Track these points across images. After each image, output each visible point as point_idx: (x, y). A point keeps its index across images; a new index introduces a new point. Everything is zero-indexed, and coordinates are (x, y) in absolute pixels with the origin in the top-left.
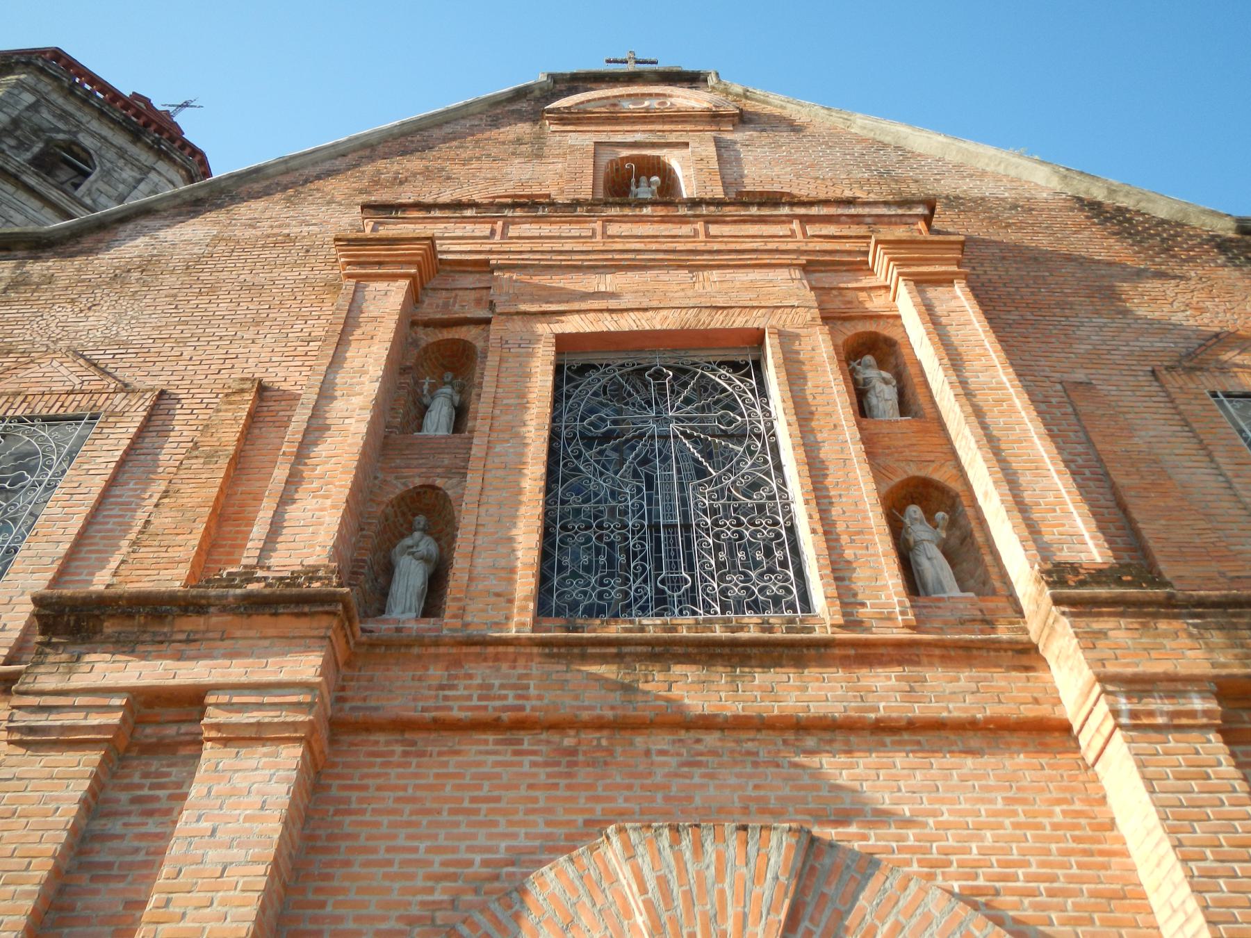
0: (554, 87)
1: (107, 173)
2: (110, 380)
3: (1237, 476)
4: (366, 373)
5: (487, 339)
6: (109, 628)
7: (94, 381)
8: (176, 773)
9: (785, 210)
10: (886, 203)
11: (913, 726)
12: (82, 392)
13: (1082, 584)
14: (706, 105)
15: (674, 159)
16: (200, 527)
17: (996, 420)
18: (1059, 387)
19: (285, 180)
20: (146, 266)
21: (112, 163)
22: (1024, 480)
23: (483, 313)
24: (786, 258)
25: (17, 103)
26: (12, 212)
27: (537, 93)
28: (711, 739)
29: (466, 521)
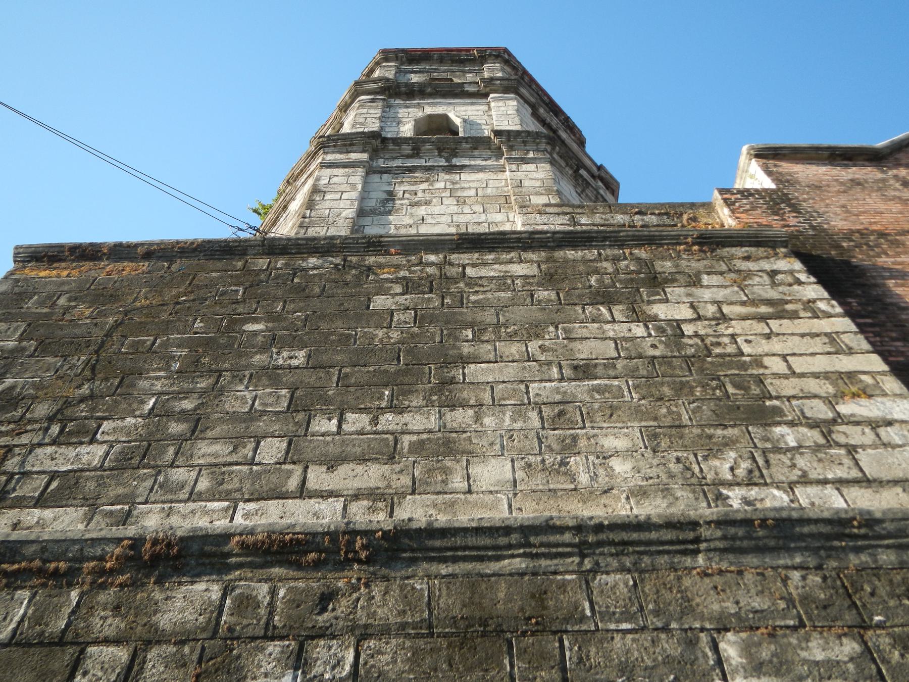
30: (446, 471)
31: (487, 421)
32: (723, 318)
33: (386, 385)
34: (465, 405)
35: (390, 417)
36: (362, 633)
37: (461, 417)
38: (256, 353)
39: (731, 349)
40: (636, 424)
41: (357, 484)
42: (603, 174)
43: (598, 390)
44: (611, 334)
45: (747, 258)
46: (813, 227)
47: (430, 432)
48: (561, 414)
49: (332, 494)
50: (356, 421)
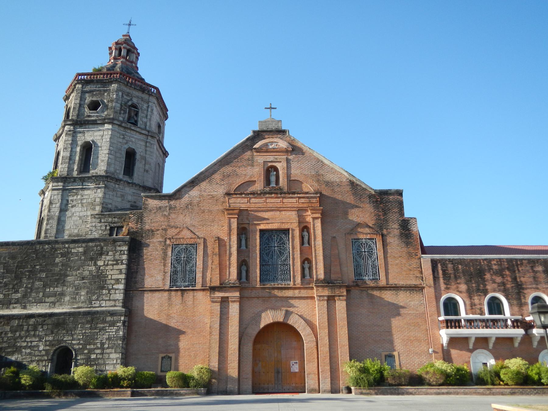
0: (254, 134)
1: (141, 109)
2: (195, 236)
3: (348, 257)
4: (234, 242)
5: (249, 227)
6: (216, 289)
7: (194, 237)
8: (227, 304)
9: (296, 195)
10: (313, 193)
11: (299, 297)
12: (192, 238)
13: (318, 283)
14: (285, 147)
15: (278, 165)
16: (218, 268)
17: (317, 252)
18: (331, 238)
19: (207, 174)
20: (191, 204)
22: (318, 263)
23: (248, 222)
25: (119, 97)
26: (132, 139)
27: (251, 138)
28: (278, 298)
30: (62, 299)
31: (68, 289)
32: (108, 265)
33: (56, 282)
34: (66, 286)
35: (56, 288)
36: (48, 325)
37: (65, 288)
38: (39, 274)
39: (105, 273)
40: (86, 290)
41: (51, 301)
42: (150, 134)
43: (84, 283)
44: (90, 269)
45: (119, 246)
46: (141, 229)
47: (60, 291)
48: (78, 288)
49: (48, 302)
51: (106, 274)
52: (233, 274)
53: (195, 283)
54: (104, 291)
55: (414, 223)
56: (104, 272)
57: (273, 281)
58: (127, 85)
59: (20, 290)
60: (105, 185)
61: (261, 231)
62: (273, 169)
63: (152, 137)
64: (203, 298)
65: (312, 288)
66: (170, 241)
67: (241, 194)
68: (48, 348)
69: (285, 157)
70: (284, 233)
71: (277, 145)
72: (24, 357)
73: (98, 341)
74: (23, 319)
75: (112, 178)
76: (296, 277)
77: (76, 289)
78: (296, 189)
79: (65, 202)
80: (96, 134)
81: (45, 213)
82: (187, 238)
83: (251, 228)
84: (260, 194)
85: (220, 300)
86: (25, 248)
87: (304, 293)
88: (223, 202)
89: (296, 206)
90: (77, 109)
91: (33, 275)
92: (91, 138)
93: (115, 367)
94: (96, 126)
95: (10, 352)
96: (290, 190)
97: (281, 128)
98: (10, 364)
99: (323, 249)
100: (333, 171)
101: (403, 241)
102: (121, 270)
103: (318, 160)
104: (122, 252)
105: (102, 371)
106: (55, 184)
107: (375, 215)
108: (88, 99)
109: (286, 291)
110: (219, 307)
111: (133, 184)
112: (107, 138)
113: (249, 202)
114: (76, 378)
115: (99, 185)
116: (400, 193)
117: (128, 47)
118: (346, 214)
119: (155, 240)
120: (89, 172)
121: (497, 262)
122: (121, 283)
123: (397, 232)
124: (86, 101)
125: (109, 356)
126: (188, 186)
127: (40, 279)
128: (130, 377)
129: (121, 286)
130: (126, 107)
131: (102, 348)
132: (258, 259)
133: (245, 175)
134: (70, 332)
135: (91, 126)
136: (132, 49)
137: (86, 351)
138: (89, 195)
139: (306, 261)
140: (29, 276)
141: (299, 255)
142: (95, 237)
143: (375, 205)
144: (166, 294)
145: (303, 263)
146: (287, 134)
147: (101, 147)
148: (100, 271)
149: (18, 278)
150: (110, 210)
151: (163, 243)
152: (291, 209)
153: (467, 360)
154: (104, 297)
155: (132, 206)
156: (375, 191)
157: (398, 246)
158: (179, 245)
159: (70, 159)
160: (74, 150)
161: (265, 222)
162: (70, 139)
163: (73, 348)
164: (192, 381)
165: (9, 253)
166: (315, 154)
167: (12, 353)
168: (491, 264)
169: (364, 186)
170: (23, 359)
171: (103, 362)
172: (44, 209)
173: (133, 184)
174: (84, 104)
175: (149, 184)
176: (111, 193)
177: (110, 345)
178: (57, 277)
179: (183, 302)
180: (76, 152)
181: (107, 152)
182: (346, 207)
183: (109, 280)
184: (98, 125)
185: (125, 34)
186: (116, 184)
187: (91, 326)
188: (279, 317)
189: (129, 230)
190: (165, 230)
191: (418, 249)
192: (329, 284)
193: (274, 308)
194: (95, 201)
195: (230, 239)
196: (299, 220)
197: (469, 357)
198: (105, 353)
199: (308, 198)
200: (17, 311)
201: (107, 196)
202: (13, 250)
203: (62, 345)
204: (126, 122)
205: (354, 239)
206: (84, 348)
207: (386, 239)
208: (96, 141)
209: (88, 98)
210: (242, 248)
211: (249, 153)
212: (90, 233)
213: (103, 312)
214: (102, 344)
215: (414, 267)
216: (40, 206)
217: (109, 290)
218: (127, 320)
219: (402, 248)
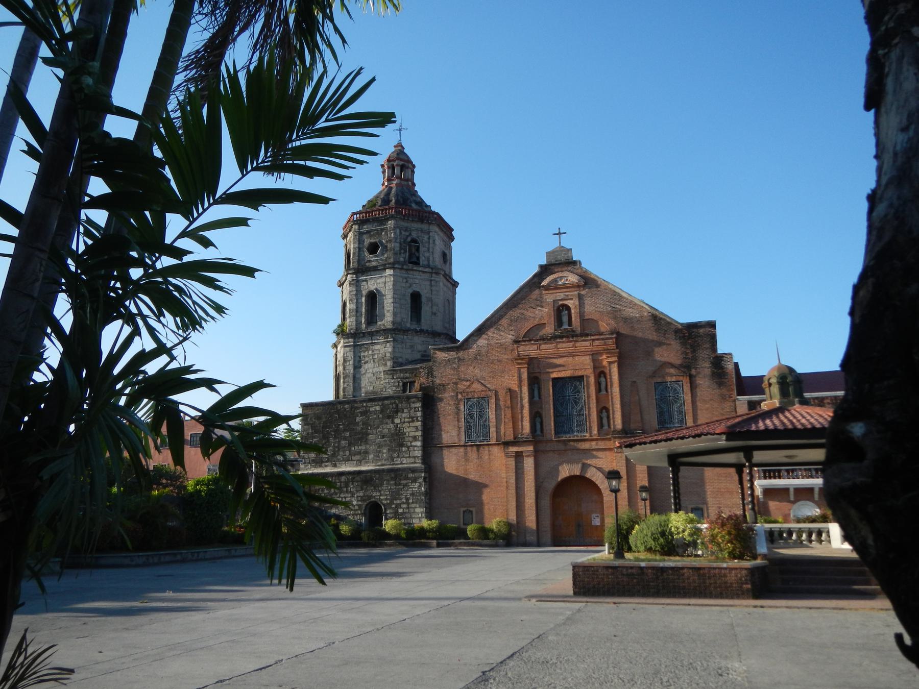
1: (422, 242)
7: (485, 389)
9: (589, 338)
10: (609, 334)
13: (615, 434)
14: (576, 281)
15: (569, 303)
16: (511, 422)
17: (614, 400)
18: (630, 383)
20: (479, 354)
21: (421, 237)
23: (539, 371)
24: (588, 353)
26: (416, 280)
29: (544, 415)
30: (366, 456)
32: (404, 422)
35: (360, 447)
36: (357, 481)
37: (368, 446)
41: (357, 459)
42: (434, 271)
43: (385, 441)
45: (413, 403)
46: (433, 384)
50: (356, 447)
51: (404, 432)
52: (526, 427)
53: (489, 437)
54: (404, 448)
55: (729, 360)
56: (402, 430)
57: (568, 432)
58: (404, 219)
59: (329, 449)
60: (393, 338)
61: (554, 379)
62: (564, 307)
63: (437, 273)
64: (497, 451)
65: (609, 439)
66: (462, 395)
67: (530, 341)
68: (360, 503)
69: (576, 293)
70: (579, 380)
71: (567, 280)
72: (341, 511)
73: (403, 497)
74: (335, 477)
75: (399, 330)
76: (593, 428)
77: (379, 447)
78: (591, 330)
79: (358, 359)
80: (379, 281)
81: (340, 369)
82: (478, 391)
83: (543, 377)
84: (550, 339)
85: (514, 454)
86: (328, 409)
87: (602, 445)
88: (513, 350)
89: (589, 350)
90: (357, 254)
91: (338, 435)
92: (375, 287)
93: (420, 521)
94: (377, 272)
95: (328, 506)
96: (583, 331)
97: (571, 258)
98: (330, 517)
99: (622, 397)
100: (632, 304)
101: (714, 382)
102: (417, 427)
103: (614, 293)
104: (417, 409)
105: (409, 524)
106: (346, 340)
107: (682, 354)
108: (367, 241)
109: (583, 443)
110: (514, 462)
111: (422, 332)
112: (390, 285)
113: (539, 348)
114: (387, 530)
115: (388, 338)
116: (712, 325)
117: (402, 163)
118: (649, 354)
119: (447, 395)
120: (376, 322)
121: (832, 400)
122: (419, 441)
123: (708, 371)
124: (365, 244)
125: (414, 510)
126: (475, 335)
127: (345, 439)
128: (434, 529)
129: (419, 444)
130: (405, 245)
131: (408, 504)
132: (552, 411)
133: (534, 318)
134: (377, 488)
135: (372, 273)
136: (406, 164)
137: (393, 506)
138: (379, 350)
139: (604, 411)
140: (335, 435)
141: (595, 404)
142: (389, 393)
143: (681, 341)
144: (462, 449)
145: (600, 412)
146: (578, 266)
147: (385, 296)
148: (398, 429)
149: (326, 437)
150: (401, 365)
151: (455, 398)
152: (584, 353)
153: (787, 512)
154: (404, 454)
155: (423, 356)
156: (682, 324)
157: (708, 388)
158: (470, 399)
159: (357, 311)
160: (359, 301)
161: (557, 369)
162: (354, 289)
163: (382, 503)
164: (490, 534)
165: (315, 414)
166: (610, 286)
167: (331, 508)
168: (824, 403)
169: (668, 320)
170: (340, 513)
171: (409, 516)
172: (339, 366)
173: (422, 331)
174: (363, 247)
175: (438, 328)
176: (399, 346)
177: (414, 500)
178: (360, 436)
179: (479, 457)
180: (362, 303)
181: (391, 301)
182: (647, 348)
183: (407, 437)
184: (380, 271)
185: (396, 143)
186: (403, 335)
187: (395, 483)
188: (576, 470)
189: (421, 385)
190: (456, 384)
191: (734, 390)
192: (626, 434)
193: (569, 462)
194: (385, 356)
195: (521, 391)
196: (594, 366)
197: (790, 510)
198: (411, 508)
199: (603, 339)
200: (328, 470)
201: (397, 350)
202: (317, 411)
203: (372, 500)
204: (407, 263)
205: (657, 383)
206: (391, 503)
207: (695, 380)
208: (379, 289)
209: (366, 240)
210: (535, 399)
211: (537, 292)
212: (384, 390)
213: (404, 469)
214: (407, 499)
215: (728, 410)
216: (334, 359)
217: (408, 447)
218: (427, 476)
219: (714, 389)
